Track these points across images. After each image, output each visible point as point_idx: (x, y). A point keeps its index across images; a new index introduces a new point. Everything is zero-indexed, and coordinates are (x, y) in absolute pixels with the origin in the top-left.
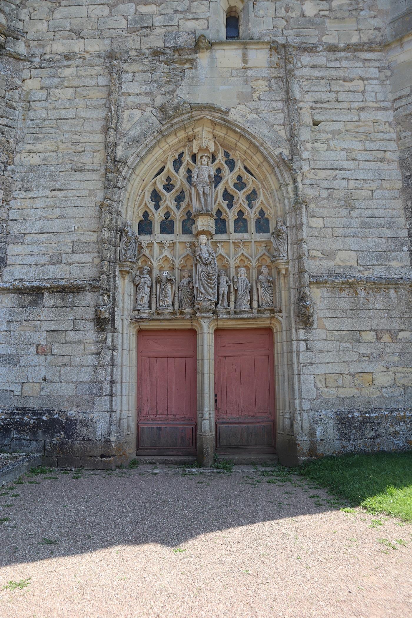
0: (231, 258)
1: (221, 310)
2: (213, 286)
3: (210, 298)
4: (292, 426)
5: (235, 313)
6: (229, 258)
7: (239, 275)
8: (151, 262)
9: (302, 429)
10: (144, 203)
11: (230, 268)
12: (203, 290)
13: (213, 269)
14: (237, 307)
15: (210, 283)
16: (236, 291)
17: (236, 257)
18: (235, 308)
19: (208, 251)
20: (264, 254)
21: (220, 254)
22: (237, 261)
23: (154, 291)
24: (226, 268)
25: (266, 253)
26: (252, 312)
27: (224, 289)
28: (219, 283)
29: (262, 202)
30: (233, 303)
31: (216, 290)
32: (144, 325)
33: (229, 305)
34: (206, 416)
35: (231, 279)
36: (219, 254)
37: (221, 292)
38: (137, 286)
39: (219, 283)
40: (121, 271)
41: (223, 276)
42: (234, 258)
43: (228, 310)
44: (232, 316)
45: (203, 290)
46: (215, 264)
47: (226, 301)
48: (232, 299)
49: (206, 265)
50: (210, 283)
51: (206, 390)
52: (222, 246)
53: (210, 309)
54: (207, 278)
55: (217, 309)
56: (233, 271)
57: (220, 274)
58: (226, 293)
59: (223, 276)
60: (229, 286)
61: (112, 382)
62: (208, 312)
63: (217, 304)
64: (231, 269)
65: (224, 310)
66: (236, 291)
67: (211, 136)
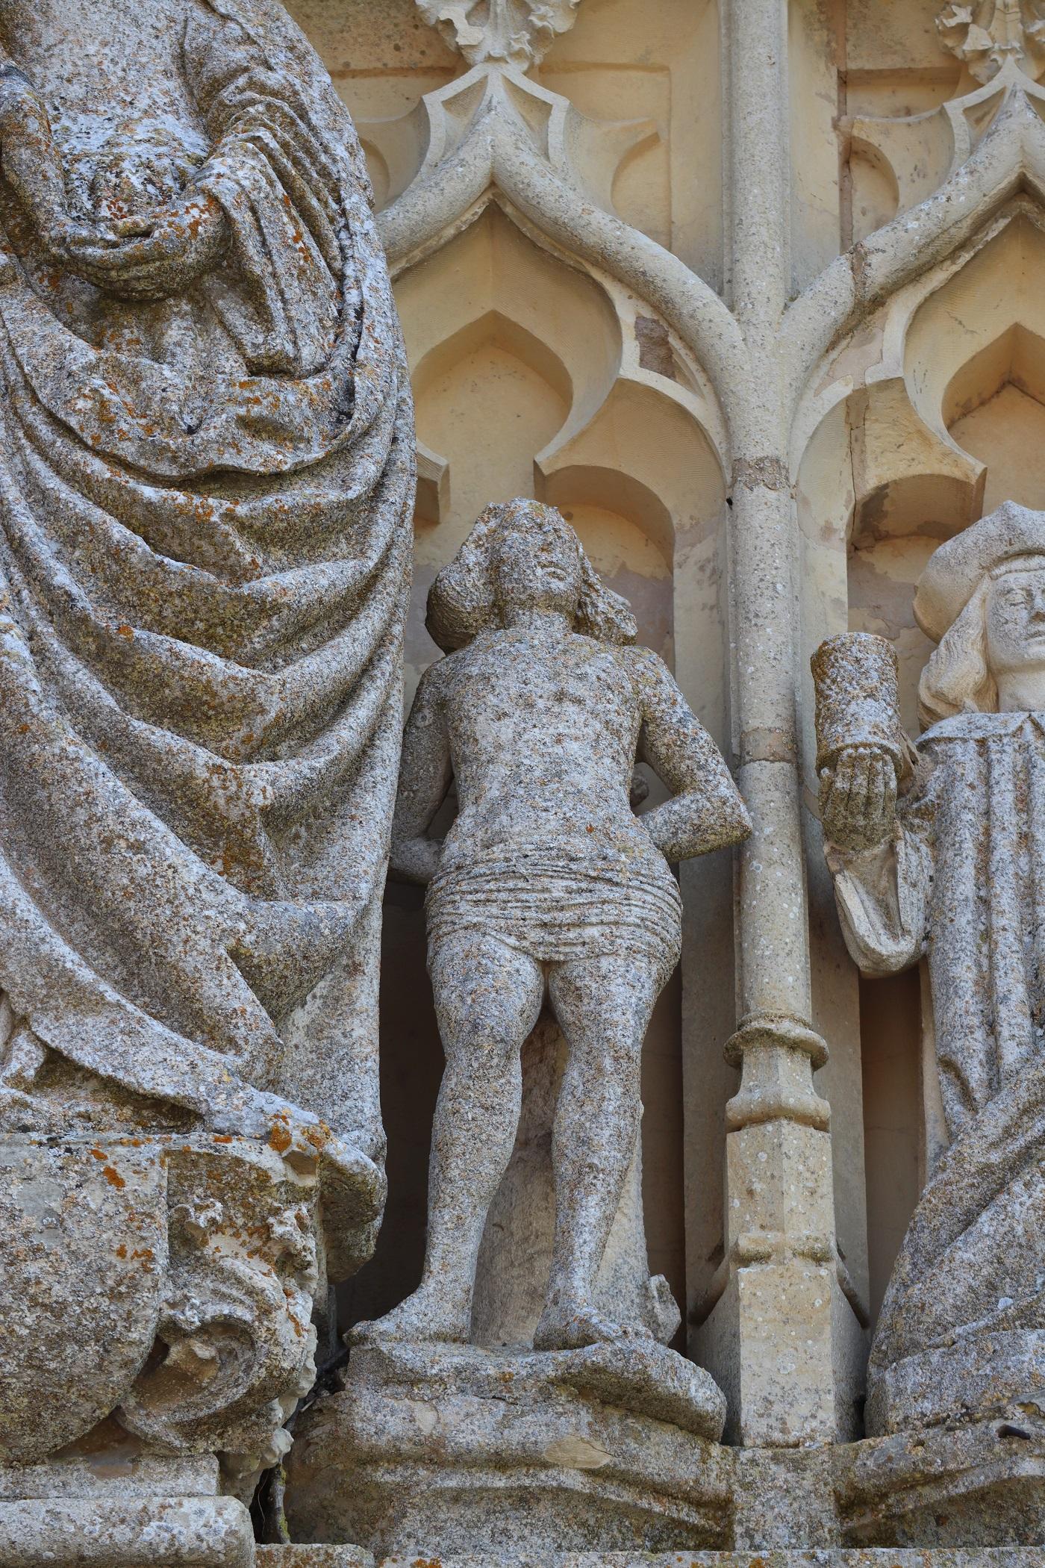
0: (761, 276)
1: (470, 1423)
2: (266, 781)
3: (161, 1060)
6: (723, 282)
7: (959, 667)
11: (729, 480)
13: (292, 399)
14: (910, 1387)
15: (191, 710)
16: (887, 1010)
17: (888, 248)
18: (861, 1415)
19: (186, 64)
21: (502, 215)
22: (922, 358)
24: (642, 523)
27: (559, 894)
28: (435, 805)
30: (820, 1291)
33: (700, 1326)
35: (763, 714)
36: (442, 194)
37: (489, 977)
39: (435, 805)
41: (545, 629)
42: (836, 287)
43: (661, 1454)
46: (348, 321)
48: (790, 1186)
50: (191, 710)
53: (156, 1372)
54: (109, 568)
55: (377, 1415)
56: (793, 574)
57: (468, 587)
58: (622, 998)
59: (545, 629)
60: (712, 880)
62: (109, 1442)
63: (375, 1261)
64: (763, 511)
65: (575, 1441)
66: (887, 1010)
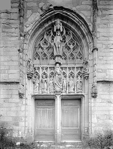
3: (60, 87)
4: (88, 131)
5: (69, 93)
8: (39, 75)
9: (92, 133)
10: (36, 53)
12: (57, 84)
15: (60, 82)
16: (69, 85)
20: (79, 72)
21: (64, 72)
22: (70, 75)
23: (40, 85)
25: (80, 72)
26: (74, 93)
29: (79, 52)
31: (62, 85)
32: (37, 97)
34: (58, 128)
38: (34, 83)
40: (28, 77)
44: (67, 94)
45: (57, 84)
47: (65, 89)
49: (59, 75)
50: (60, 82)
51: (58, 119)
52: (64, 69)
61: (26, 117)
67: (61, 24)
